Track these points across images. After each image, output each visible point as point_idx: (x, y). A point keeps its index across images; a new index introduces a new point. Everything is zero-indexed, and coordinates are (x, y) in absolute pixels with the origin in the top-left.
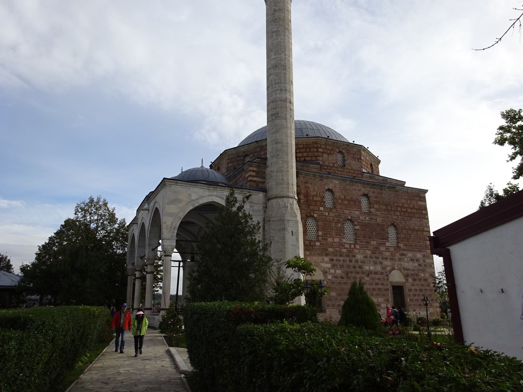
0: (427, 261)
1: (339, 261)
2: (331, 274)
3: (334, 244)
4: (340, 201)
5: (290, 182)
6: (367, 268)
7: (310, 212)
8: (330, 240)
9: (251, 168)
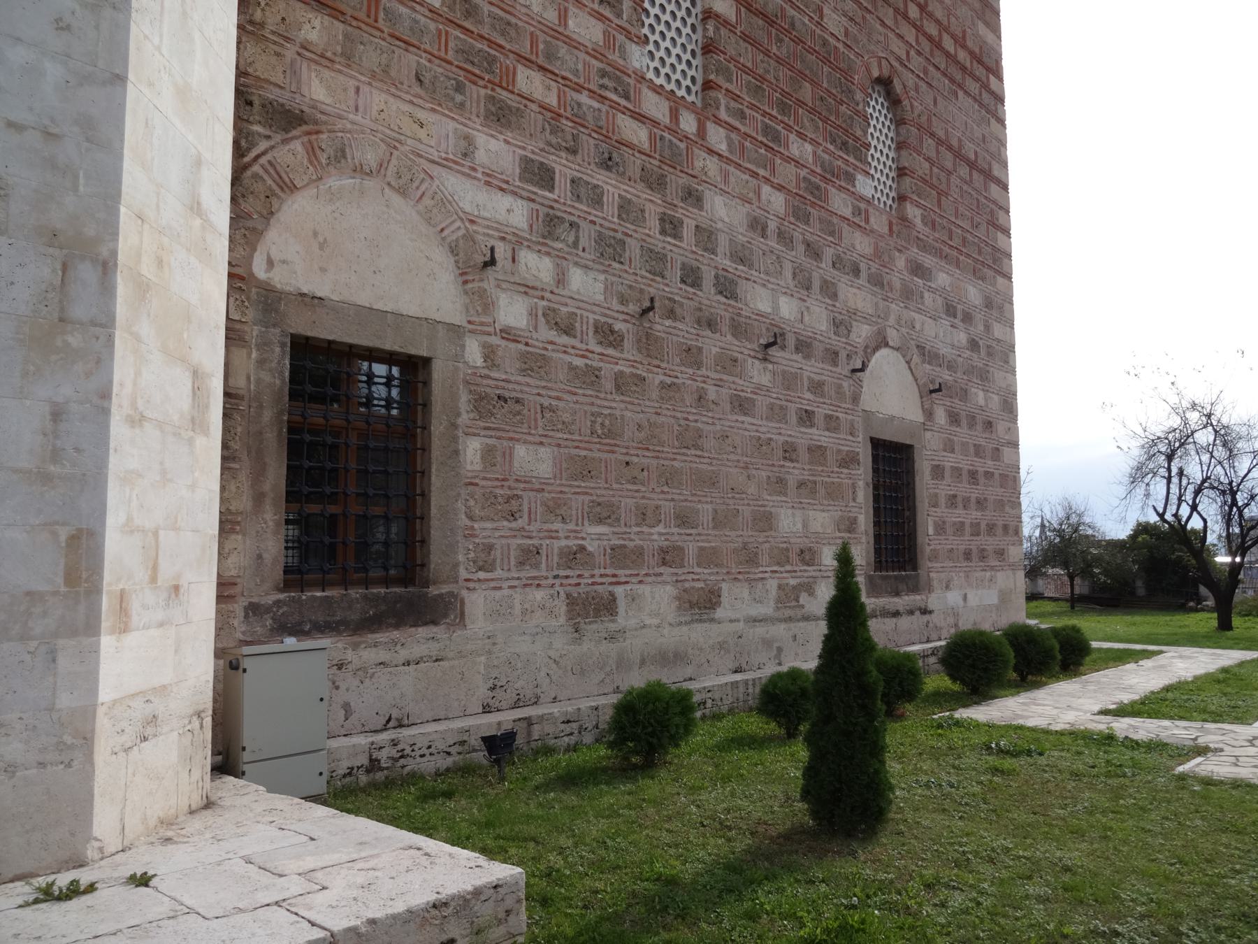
0: (998, 331)
2: (527, 289)
3: (563, 51)
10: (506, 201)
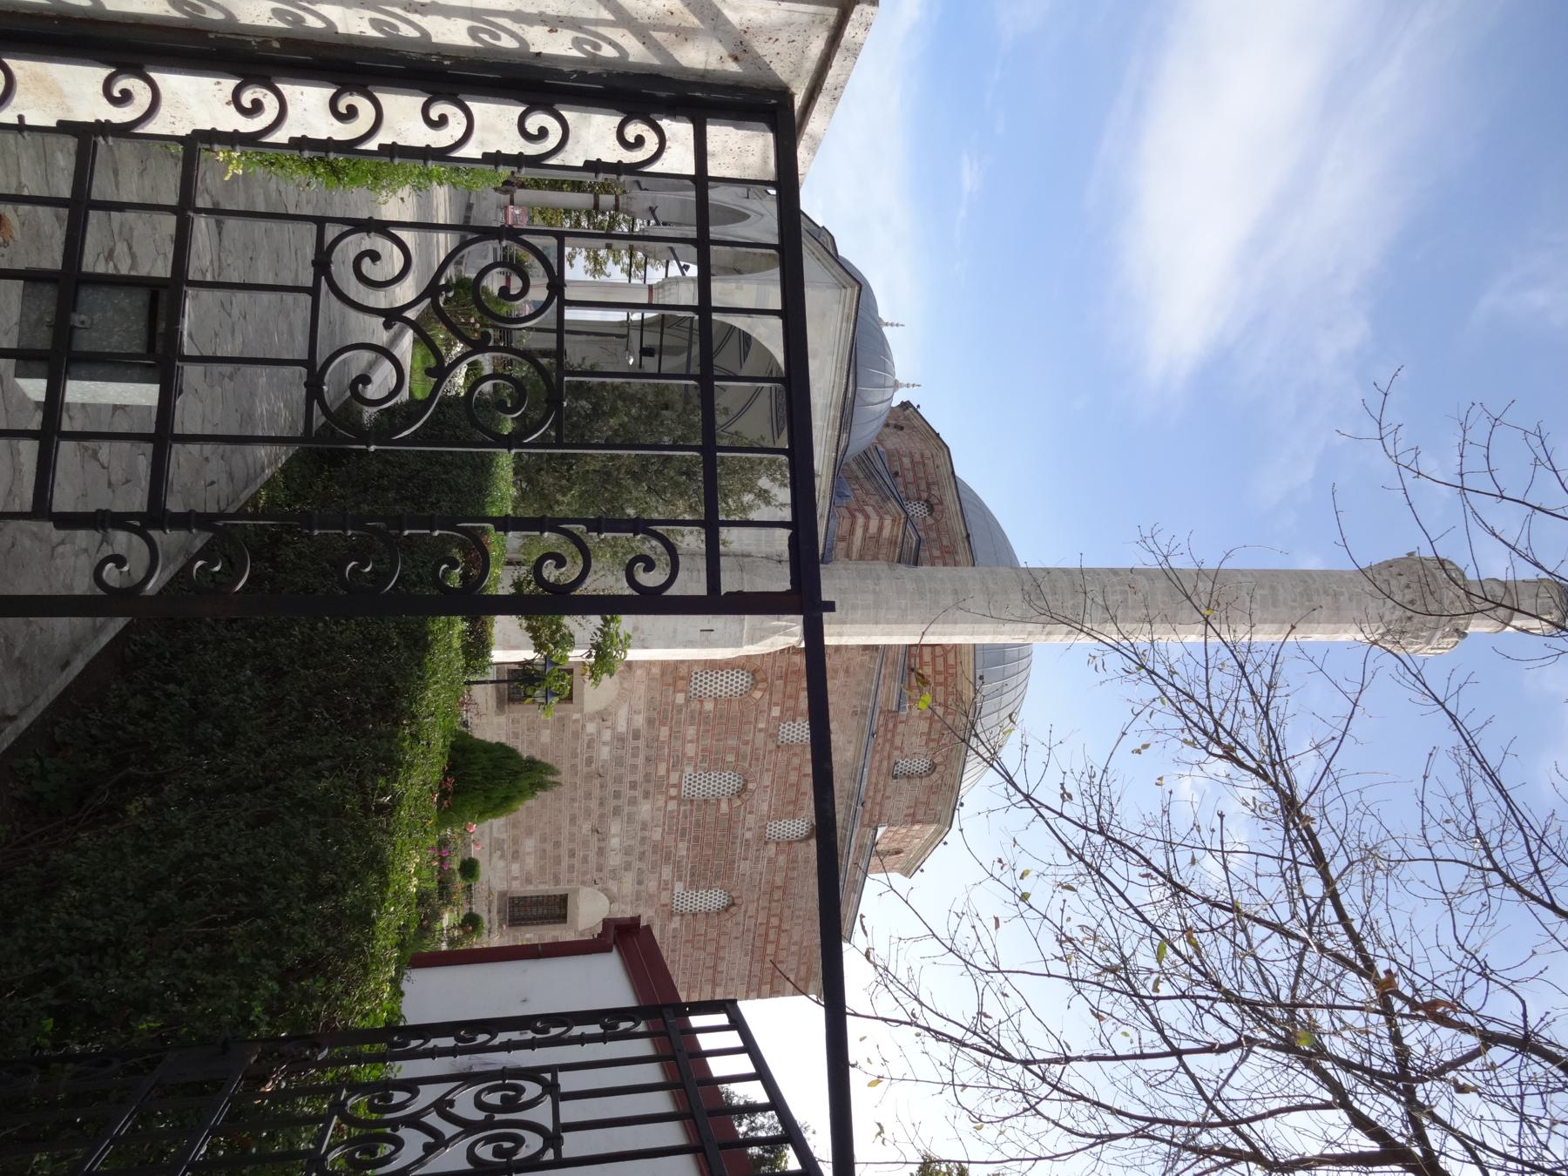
1: (635, 756)
2: (599, 732)
5: (847, 628)
6: (615, 827)
7: (765, 680)
8: (691, 732)
9: (888, 522)
10: (624, 724)
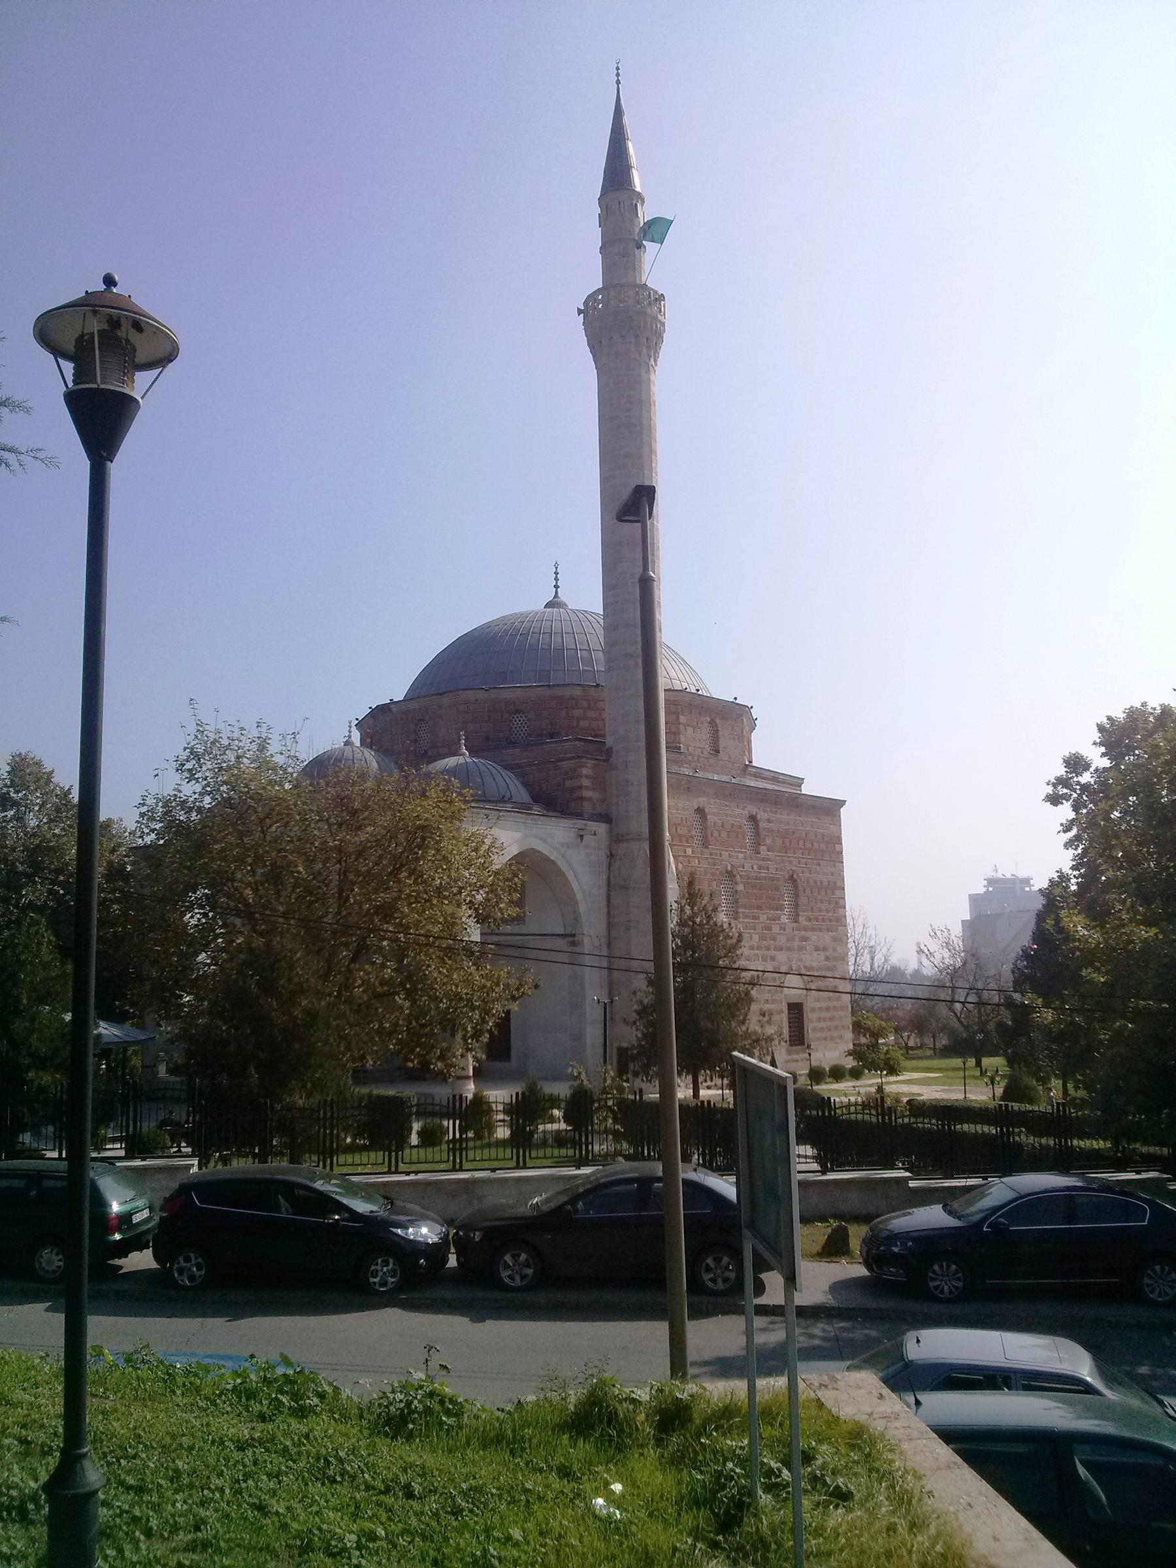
0: (839, 949)
4: (716, 834)
